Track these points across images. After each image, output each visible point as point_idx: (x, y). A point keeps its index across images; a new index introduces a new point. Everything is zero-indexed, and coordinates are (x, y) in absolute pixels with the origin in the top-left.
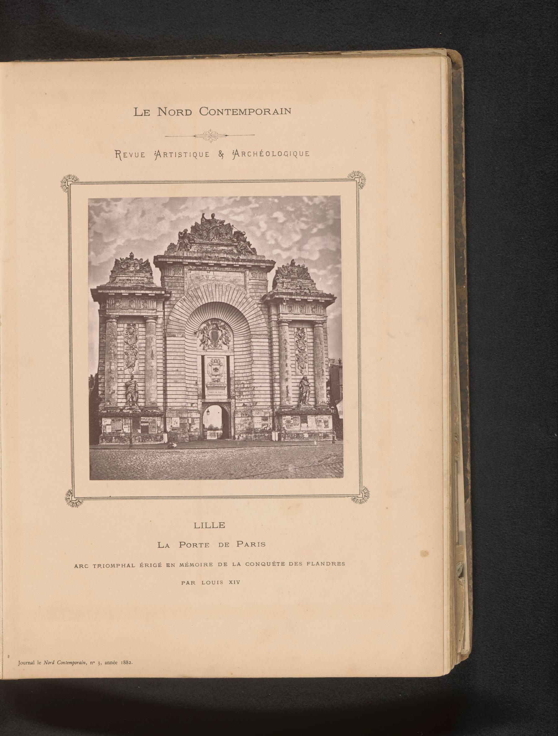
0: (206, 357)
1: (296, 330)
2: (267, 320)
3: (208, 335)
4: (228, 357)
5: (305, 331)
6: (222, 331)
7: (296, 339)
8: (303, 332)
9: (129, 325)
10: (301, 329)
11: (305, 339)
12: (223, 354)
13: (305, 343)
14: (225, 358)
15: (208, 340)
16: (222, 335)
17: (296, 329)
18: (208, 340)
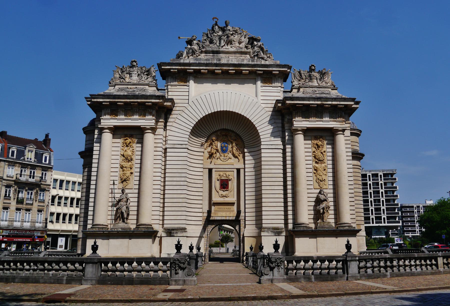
0: (214, 170)
2: (280, 129)
3: (217, 147)
4: (238, 170)
11: (324, 149)
13: (324, 153)
15: (217, 153)
18: (217, 153)
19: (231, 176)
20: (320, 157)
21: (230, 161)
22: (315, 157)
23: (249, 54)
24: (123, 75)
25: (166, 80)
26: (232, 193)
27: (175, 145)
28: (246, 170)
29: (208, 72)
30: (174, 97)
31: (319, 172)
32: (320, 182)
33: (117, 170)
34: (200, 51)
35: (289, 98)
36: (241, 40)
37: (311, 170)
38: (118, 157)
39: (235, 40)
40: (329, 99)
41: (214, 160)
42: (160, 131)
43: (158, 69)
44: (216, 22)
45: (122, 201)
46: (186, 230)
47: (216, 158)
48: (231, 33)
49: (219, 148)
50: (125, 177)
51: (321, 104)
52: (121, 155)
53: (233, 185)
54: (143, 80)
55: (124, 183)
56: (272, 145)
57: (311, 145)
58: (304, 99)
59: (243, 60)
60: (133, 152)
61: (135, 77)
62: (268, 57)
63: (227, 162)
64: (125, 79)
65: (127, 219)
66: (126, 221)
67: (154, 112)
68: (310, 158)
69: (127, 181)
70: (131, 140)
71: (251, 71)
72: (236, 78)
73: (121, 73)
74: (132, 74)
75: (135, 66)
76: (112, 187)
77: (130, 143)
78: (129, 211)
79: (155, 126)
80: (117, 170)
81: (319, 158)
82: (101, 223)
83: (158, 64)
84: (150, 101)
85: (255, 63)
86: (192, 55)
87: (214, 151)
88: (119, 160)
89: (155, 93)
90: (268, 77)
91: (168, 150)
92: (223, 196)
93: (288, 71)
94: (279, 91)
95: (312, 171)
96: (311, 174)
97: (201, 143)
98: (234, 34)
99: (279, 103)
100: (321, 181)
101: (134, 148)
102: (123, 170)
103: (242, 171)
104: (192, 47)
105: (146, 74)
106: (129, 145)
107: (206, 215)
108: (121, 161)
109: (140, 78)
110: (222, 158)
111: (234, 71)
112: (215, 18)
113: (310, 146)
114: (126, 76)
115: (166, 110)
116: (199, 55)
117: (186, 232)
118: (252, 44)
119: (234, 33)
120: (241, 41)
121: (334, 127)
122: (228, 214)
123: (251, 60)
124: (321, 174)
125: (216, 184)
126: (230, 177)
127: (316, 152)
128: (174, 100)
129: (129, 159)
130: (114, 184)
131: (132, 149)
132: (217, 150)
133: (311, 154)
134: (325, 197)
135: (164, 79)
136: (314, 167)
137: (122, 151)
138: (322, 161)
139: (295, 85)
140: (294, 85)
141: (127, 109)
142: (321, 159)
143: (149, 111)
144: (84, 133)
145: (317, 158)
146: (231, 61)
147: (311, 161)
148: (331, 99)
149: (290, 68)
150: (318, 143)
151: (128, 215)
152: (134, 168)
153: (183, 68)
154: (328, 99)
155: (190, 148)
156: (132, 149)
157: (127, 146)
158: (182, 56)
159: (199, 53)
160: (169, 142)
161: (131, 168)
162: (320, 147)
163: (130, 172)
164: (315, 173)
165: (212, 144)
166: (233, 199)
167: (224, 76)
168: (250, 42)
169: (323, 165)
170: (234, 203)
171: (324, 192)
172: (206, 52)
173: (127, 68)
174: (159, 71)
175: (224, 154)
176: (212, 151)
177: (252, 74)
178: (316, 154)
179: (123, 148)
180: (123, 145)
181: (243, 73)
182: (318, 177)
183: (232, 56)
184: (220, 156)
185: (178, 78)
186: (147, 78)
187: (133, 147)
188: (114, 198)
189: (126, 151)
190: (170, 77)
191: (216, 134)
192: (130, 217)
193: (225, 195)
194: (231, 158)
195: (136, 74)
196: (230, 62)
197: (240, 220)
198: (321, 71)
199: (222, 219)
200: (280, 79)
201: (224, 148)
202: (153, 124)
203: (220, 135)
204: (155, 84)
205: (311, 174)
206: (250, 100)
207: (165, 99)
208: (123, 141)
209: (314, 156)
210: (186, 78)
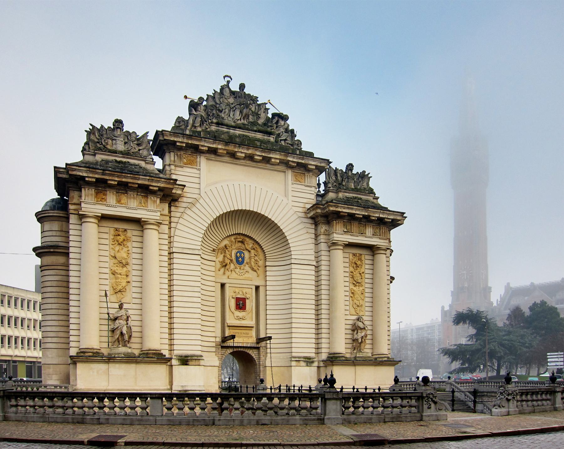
1: (351, 257)
2: (313, 241)
5: (363, 259)
8: (360, 259)
9: (116, 230)
11: (362, 270)
13: (362, 275)
17: (351, 255)
19: (249, 294)
20: (359, 278)
22: (353, 277)
23: (273, 136)
24: (103, 140)
28: (268, 288)
33: (107, 276)
34: (210, 121)
38: (107, 259)
42: (165, 228)
45: (122, 319)
47: (230, 270)
50: (119, 288)
52: (111, 256)
54: (133, 152)
55: (119, 295)
57: (348, 264)
61: (120, 146)
64: (106, 146)
65: (129, 342)
66: (128, 345)
69: (123, 293)
73: (99, 136)
74: (115, 140)
75: (120, 128)
76: (104, 299)
78: (131, 332)
80: (107, 276)
82: (95, 347)
87: (228, 261)
88: (109, 263)
95: (348, 295)
101: (129, 249)
102: (116, 277)
104: (198, 113)
106: (122, 244)
108: (112, 265)
110: (237, 270)
112: (228, 76)
114: (107, 141)
115: (170, 200)
118: (277, 122)
127: (355, 273)
129: (124, 263)
130: (106, 295)
131: (127, 249)
137: (111, 250)
145: (355, 280)
147: (348, 283)
150: (357, 263)
151: (130, 337)
152: (130, 276)
156: (127, 249)
157: (119, 244)
161: (127, 276)
163: (127, 281)
165: (225, 251)
172: (218, 124)
173: (108, 131)
178: (354, 276)
179: (114, 248)
180: (113, 243)
184: (235, 268)
185: (184, 157)
186: (139, 150)
187: (128, 247)
188: (108, 314)
189: (118, 251)
190: (172, 154)
192: (133, 340)
194: (248, 272)
195: (122, 141)
208: (112, 237)
209: (351, 276)
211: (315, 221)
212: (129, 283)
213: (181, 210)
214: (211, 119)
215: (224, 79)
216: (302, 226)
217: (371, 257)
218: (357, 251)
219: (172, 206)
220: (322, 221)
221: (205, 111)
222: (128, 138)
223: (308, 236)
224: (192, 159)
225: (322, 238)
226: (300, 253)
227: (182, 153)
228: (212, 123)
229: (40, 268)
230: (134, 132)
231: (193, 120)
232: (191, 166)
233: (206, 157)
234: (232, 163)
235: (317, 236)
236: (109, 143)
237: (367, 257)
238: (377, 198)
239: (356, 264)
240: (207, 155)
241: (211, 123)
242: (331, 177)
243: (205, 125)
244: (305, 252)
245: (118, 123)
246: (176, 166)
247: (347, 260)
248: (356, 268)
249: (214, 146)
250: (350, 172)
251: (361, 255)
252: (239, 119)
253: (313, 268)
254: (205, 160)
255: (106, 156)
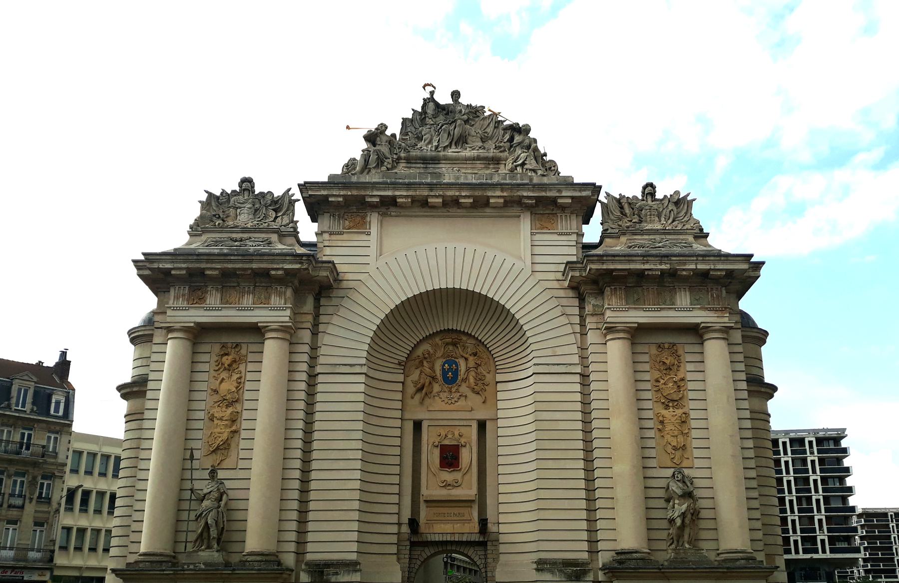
0: (425, 425)
1: (654, 350)
2: (577, 328)
3: (432, 368)
4: (482, 425)
5: (680, 352)
6: (466, 359)
7: (657, 374)
9: (224, 346)
10: (666, 346)
11: (681, 375)
12: (467, 415)
14: (475, 425)
16: (468, 370)
21: (462, 403)
23: (504, 162)
25: (319, 221)
26: (467, 477)
27: (338, 366)
29: (413, 202)
30: (336, 260)
31: (669, 427)
32: (673, 452)
34: (395, 156)
35: (596, 258)
36: (486, 132)
37: (650, 424)
39: (473, 133)
40: (689, 259)
41: (428, 401)
43: (301, 199)
44: (432, 93)
46: (358, 567)
48: (465, 117)
49: (438, 373)
51: (671, 271)
53: (468, 456)
54: (265, 223)
56: (558, 364)
58: (630, 258)
59: (491, 176)
60: (240, 382)
62: (546, 170)
63: (457, 404)
67: (289, 292)
68: (648, 395)
70: (235, 356)
71: (508, 199)
72: (474, 217)
75: (249, 191)
77: (234, 361)
79: (290, 324)
81: (669, 394)
83: (299, 185)
84: (281, 266)
85: (519, 181)
86: (377, 167)
89: (291, 249)
90: (547, 212)
91: (320, 378)
92: (447, 485)
93: (592, 197)
94: (574, 243)
96: (651, 433)
97: (397, 362)
98: (471, 120)
99: (573, 269)
100: (675, 448)
103: (489, 425)
104: (378, 147)
105: (272, 209)
107: (405, 529)
109: (259, 218)
111: (471, 200)
112: (428, 85)
113: (647, 367)
115: (317, 289)
116: (393, 167)
117: (360, 570)
118: (511, 139)
119: (471, 117)
120: (486, 135)
121: (702, 323)
122: (458, 528)
123: (510, 177)
124: (676, 433)
125: (431, 457)
126: (463, 441)
128: (336, 265)
132: (434, 378)
133: (648, 386)
134: (686, 487)
135: (314, 220)
136: (657, 415)
138: (676, 401)
139: (610, 229)
140: (607, 230)
141: (228, 285)
142: (675, 397)
143: (279, 289)
144: (133, 341)
145: (664, 395)
146: (464, 179)
147: (651, 402)
148: (695, 258)
149: (596, 189)
150: (665, 361)
153: (355, 193)
154: (687, 258)
155: (372, 373)
156: (238, 376)
158: (355, 169)
159: (393, 161)
160: (322, 360)
162: (671, 369)
164: (659, 430)
165: (423, 363)
166: (469, 491)
167: (449, 212)
168: (507, 137)
169: (679, 412)
170: (472, 501)
171: (683, 476)
174: (302, 201)
175: (450, 386)
176: (422, 381)
177: (513, 207)
181: (491, 205)
182: (670, 439)
183: (466, 168)
186: (276, 217)
190: (327, 215)
191: (430, 342)
193: (451, 483)
196: (462, 180)
197: (486, 542)
198: (669, 197)
199: (445, 539)
200: (574, 217)
201: (450, 373)
202: (287, 319)
203: (440, 342)
204: (292, 230)
205: (651, 433)
206: (507, 266)
207: (314, 263)
209: (656, 389)
210: (364, 218)
211: (579, 293)
212: (236, 434)
213: (335, 301)
214: (396, 154)
215: (425, 89)
216: (554, 303)
217: (697, 348)
218: (667, 339)
219: (322, 297)
220: (589, 291)
221: (389, 143)
222: (260, 203)
223: (564, 320)
224: (359, 219)
225: (590, 322)
226: (549, 352)
227: (342, 212)
228: (399, 158)
229: (125, 416)
230: (269, 192)
231: (365, 160)
232: (356, 230)
233: (381, 213)
234: (427, 216)
235: (582, 318)
236: (231, 214)
237: (688, 348)
238: (707, 235)
239: (664, 363)
240: (383, 210)
241: (397, 159)
242: (611, 211)
243: (386, 164)
244: (559, 351)
245: (247, 183)
246: (331, 234)
247: (646, 358)
248: (665, 372)
249: (389, 193)
250: (649, 198)
251: (674, 345)
252: (447, 146)
253: (577, 378)
254: (380, 217)
255: (218, 234)
